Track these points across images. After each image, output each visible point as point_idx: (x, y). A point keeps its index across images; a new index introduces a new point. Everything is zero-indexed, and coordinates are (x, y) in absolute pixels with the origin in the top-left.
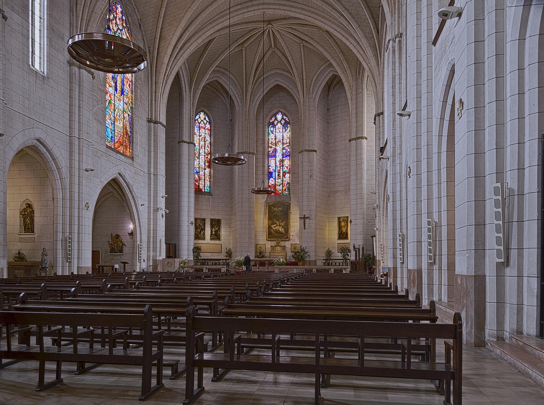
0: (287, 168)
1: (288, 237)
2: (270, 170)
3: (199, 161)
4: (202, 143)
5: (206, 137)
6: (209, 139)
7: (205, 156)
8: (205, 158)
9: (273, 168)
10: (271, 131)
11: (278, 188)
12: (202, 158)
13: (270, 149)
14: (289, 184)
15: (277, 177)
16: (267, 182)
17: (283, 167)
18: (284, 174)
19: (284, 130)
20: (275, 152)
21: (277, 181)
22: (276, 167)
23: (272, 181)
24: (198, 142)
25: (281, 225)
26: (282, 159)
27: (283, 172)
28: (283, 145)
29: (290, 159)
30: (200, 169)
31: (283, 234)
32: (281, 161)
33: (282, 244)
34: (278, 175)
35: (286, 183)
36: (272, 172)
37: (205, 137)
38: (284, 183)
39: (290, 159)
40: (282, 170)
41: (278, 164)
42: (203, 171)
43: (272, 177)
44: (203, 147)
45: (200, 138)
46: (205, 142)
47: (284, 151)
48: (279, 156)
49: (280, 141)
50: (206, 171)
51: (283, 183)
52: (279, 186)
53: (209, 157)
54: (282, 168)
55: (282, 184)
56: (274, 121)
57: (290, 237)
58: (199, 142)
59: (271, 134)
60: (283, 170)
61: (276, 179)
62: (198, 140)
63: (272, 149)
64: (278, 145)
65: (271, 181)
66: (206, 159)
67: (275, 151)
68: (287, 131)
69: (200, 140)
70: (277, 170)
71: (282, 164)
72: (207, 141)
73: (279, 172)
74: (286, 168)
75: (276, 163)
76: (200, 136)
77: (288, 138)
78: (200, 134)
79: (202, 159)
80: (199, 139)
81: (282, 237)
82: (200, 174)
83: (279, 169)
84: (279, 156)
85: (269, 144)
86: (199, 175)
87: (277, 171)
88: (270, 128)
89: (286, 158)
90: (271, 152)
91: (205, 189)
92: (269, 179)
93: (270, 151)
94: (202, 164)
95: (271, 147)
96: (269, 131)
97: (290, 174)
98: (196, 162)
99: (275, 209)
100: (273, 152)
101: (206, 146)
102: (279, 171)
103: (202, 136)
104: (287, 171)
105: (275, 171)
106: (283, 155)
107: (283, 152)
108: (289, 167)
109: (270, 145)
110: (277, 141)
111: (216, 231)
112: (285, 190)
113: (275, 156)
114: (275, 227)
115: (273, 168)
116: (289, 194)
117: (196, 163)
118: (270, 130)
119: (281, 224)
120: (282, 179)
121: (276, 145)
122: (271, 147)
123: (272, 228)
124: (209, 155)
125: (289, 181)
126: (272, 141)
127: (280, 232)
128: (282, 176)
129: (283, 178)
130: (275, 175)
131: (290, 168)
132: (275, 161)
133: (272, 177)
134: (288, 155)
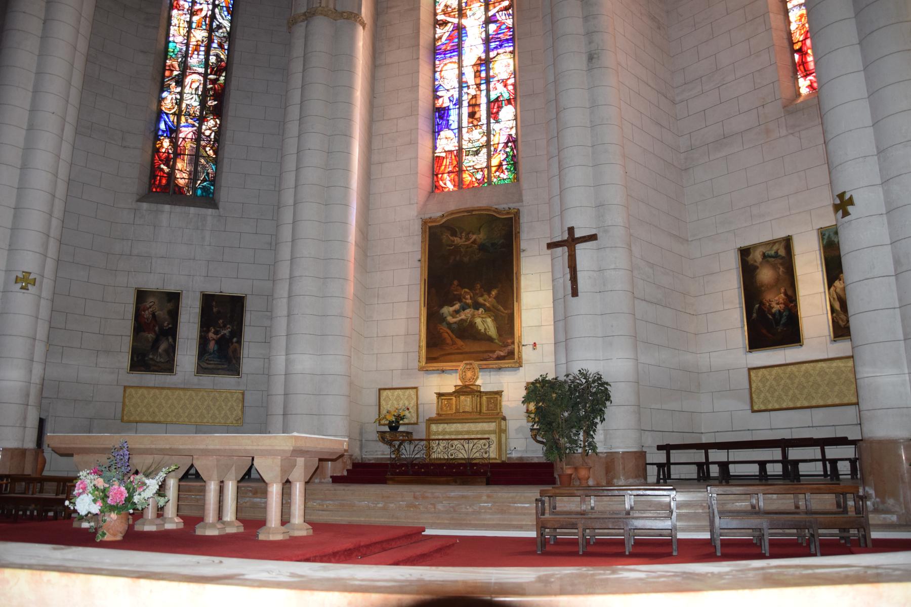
0: (505, 86)
1: (511, 354)
2: (440, 100)
3: (181, 94)
4: (199, 35)
5: (218, 16)
6: (227, 24)
7: (205, 75)
8: (205, 85)
9: (451, 92)
11: (468, 161)
12: (194, 81)
13: (439, 31)
14: (515, 141)
16: (428, 143)
17: (488, 82)
18: (494, 107)
20: (460, 38)
21: (466, 136)
22: (461, 88)
24: (183, 32)
25: (483, 306)
26: (483, 56)
27: (489, 102)
28: (487, 9)
29: (512, 52)
30: (183, 118)
31: (490, 339)
32: (481, 65)
33: (486, 381)
34: (472, 115)
35: (504, 139)
36: (448, 109)
37: (213, 17)
38: (494, 140)
39: (512, 52)
40: (484, 93)
41: (469, 77)
42: (193, 126)
43: (448, 126)
44: (202, 49)
45: (195, 19)
46: (211, 30)
47: (492, 27)
48: (473, 49)
50: (204, 127)
51: (488, 141)
52: (477, 153)
53: (222, 78)
54: (483, 87)
55: (488, 144)
57: (519, 352)
58: (189, 32)
60: (488, 95)
61: (464, 131)
62: (186, 25)
63: (450, 27)
64: (469, 13)
66: (210, 86)
67: (460, 30)
69: (194, 25)
70: (465, 97)
71: (483, 74)
72: (220, 27)
73: (474, 105)
74: (500, 87)
75: (461, 74)
76: (192, 13)
78: (197, 7)
79: (195, 86)
80: (190, 23)
81: (486, 356)
82: (182, 135)
83: (473, 91)
84: (473, 49)
85: (435, 14)
86: (177, 138)
87: (465, 104)
89: (500, 51)
90: (443, 40)
91: (195, 189)
92: (435, 133)
93: (440, 38)
94: (192, 101)
95: (445, 23)
97: (516, 108)
98: (169, 97)
99: (457, 240)
100: (450, 38)
101: (215, 45)
102: (473, 102)
103: (203, 14)
104: (506, 96)
105: (459, 103)
106: (487, 41)
108: (512, 81)
109: (440, 17)
111: (224, 343)
112: (500, 165)
113: (458, 49)
114: (457, 312)
115: (449, 94)
116: (517, 179)
117: (169, 99)
119: (481, 300)
120: (485, 127)
121: (461, 13)
122: (445, 23)
123: (443, 319)
124: (224, 74)
125: (513, 132)
127: (478, 331)
129: (488, 123)
130: (460, 116)
131: (514, 85)
132: (460, 67)
133: (448, 126)
134: (507, 41)
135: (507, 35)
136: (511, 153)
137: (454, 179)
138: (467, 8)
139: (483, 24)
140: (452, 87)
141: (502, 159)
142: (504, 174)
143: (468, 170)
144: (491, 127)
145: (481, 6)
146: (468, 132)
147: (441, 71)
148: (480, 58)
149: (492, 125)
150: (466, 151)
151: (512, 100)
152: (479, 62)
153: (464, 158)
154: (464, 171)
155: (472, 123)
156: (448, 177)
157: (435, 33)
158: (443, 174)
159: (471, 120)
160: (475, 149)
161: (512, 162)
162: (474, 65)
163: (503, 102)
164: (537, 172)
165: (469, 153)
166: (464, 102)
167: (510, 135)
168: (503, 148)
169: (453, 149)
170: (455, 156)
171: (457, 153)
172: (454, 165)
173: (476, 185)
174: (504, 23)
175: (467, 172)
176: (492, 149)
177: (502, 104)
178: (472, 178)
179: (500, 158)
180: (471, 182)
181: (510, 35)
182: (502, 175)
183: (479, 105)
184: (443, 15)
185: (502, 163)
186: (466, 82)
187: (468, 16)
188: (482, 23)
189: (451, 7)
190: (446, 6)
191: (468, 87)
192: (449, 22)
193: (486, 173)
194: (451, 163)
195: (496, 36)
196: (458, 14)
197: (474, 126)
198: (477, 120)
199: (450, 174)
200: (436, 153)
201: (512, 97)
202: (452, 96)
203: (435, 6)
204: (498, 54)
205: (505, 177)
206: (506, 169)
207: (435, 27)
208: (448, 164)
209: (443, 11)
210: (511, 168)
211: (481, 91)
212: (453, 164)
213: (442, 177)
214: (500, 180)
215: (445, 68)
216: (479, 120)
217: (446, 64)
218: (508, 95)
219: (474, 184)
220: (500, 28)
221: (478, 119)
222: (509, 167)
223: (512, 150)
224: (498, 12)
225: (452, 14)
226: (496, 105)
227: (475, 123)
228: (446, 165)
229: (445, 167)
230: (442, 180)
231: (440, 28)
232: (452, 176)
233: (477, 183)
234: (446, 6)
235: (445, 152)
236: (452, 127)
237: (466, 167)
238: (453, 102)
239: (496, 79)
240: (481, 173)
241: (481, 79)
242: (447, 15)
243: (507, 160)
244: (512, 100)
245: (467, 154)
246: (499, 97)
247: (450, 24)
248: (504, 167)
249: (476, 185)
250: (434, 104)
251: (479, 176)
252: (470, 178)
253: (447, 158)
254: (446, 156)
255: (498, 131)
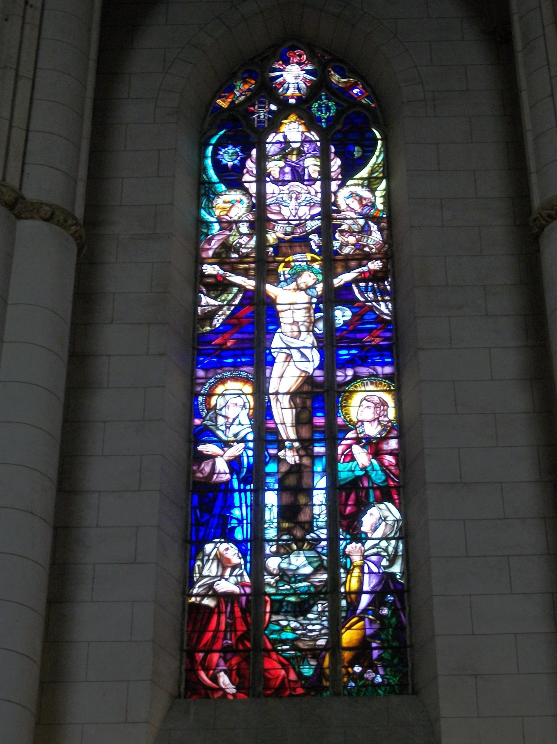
9: (236, 450)
10: (218, 166)
15: (271, 533)
19: (336, 163)
21: (273, 563)
23: (222, 561)
49: (304, 240)
56: (250, 101)
59: (222, 187)
61: (269, 549)
65: (211, 569)
68: (364, 173)
77: (377, 220)
83: (291, 457)
85: (200, 261)
88: (209, 151)
89: (363, 370)
93: (210, 316)
96: (204, 170)
102: (291, 481)
107: (329, 320)
109: (210, 269)
110: (271, 238)
118: (209, 162)
125: (397, 569)
126: (234, 239)
128: (322, 520)
135: (378, 337)
136: (394, 620)
137: (238, 669)
138: (278, 259)
139: (317, 304)
140: (239, 438)
141: (369, 632)
142: (377, 673)
143: (277, 651)
144: (342, 547)
145: (313, 260)
146: (276, 554)
147: (209, 395)
148: (309, 379)
149: (343, 543)
150: (273, 601)
151: (394, 491)
152: (306, 388)
153: (268, 616)
154: (268, 651)
155: (288, 531)
156: (222, 662)
157: (197, 302)
158: (208, 651)
159: (286, 525)
160: (292, 599)
161: (395, 644)
162: (293, 395)
163: (371, 492)
164: (476, 676)
165: (281, 607)
166: (269, 480)
167: (393, 575)
168: (369, 604)
169: (237, 590)
170: (243, 611)
171: (248, 601)
172: (239, 633)
173: (300, 691)
174: (371, 309)
175: (274, 656)
176: (344, 603)
177: (367, 496)
178: (287, 673)
179: (365, 629)
180: (285, 680)
181: (386, 339)
182: (370, 675)
183: (309, 491)
184: (217, 267)
185: (370, 643)
186: (276, 432)
187: (282, 278)
188: (314, 300)
189: (237, 251)
190: (226, 247)
191: (280, 444)
192: (234, 285)
193: (326, 663)
194: (232, 627)
195: (351, 336)
196: (257, 270)
197: (296, 540)
198: (303, 528)
199: (229, 656)
200: (191, 595)
201: (392, 484)
202: (239, 458)
203: (198, 242)
204: (356, 377)
205: (379, 679)
206: (380, 658)
207: (196, 292)
208: (223, 627)
209: (216, 255)
210: (393, 658)
211: (314, 457)
212: (236, 631)
213: (205, 658)
214: (364, 686)
215: (220, 389)
216: (309, 527)
217: (222, 381)
218: (384, 478)
219: (295, 689)
220: (362, 319)
221: (307, 526)
222: (386, 656)
223: (395, 612)
224: (356, 281)
225: (242, 266)
226: (353, 496)
227: (298, 533)
228: (217, 631)
229: (214, 637)
230: (207, 670)
231: (208, 295)
232: (234, 662)
233: (302, 687)
234: (226, 247)
235: (216, 595)
236: (238, 535)
237: (274, 642)
238: (238, 474)
239: (351, 435)
240: (313, 663)
241: (314, 429)
242: (227, 267)
243: (383, 637)
244: (394, 491)
245: (276, 608)
246: (358, 479)
247: (235, 290)
248: (375, 653)
249: (300, 691)
250: (190, 473)
251: (307, 671)
252: (283, 672)
253: (220, 613)
254: (218, 606)
255: (357, 559)
